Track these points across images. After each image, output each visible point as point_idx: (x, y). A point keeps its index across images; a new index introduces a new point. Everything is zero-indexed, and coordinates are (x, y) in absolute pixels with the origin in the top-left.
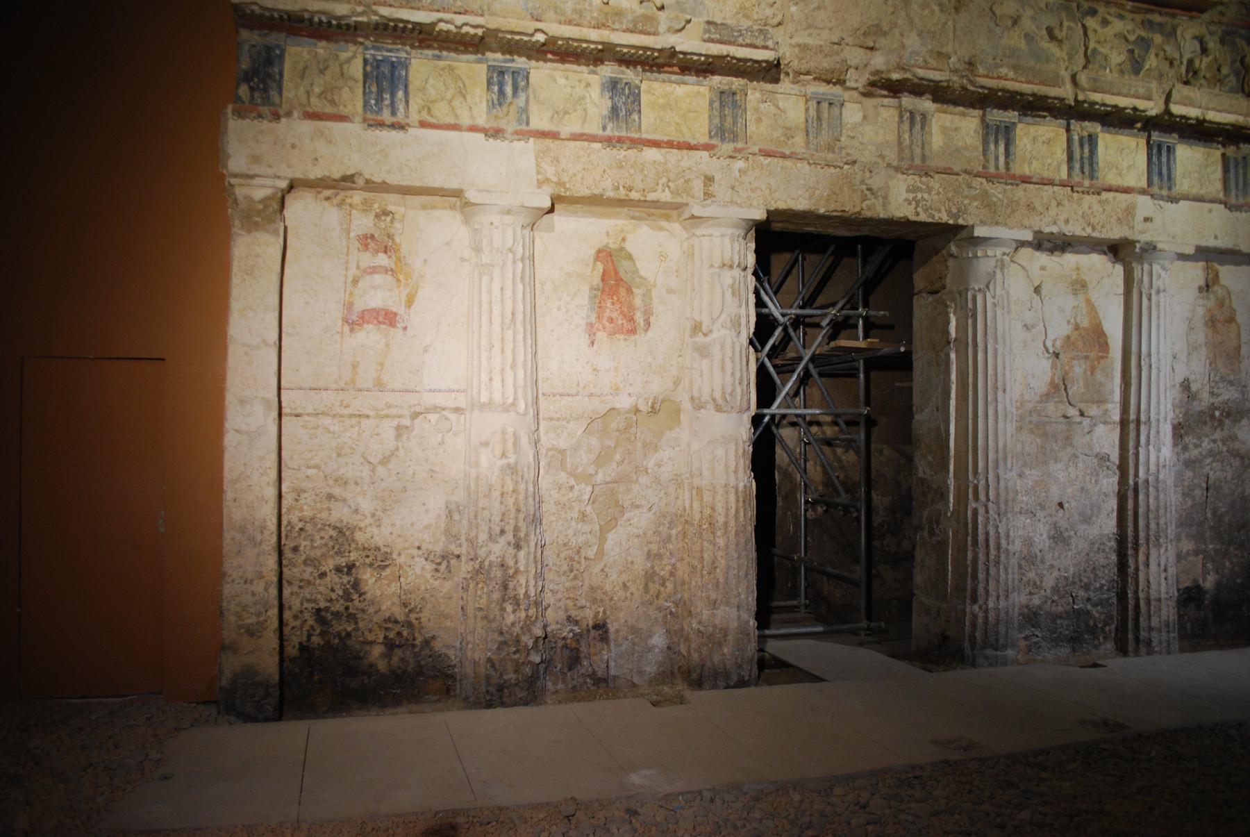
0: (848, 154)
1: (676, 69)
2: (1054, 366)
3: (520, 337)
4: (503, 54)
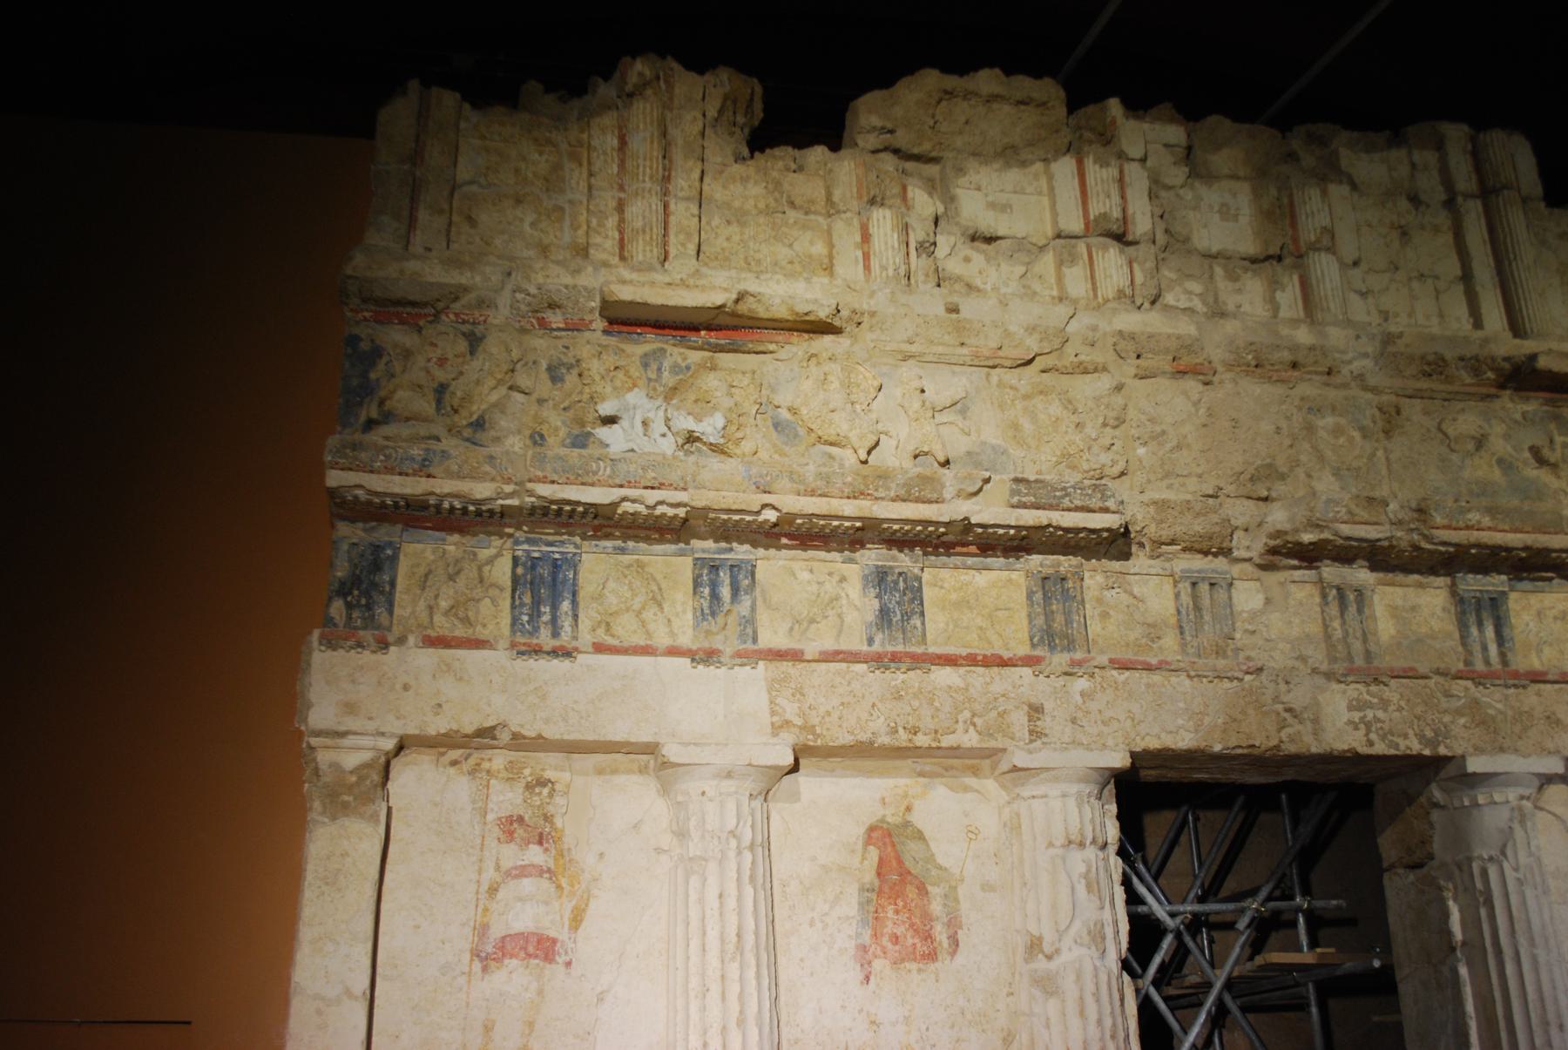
0: (1248, 658)
1: (973, 549)
3: (751, 974)
4: (716, 541)
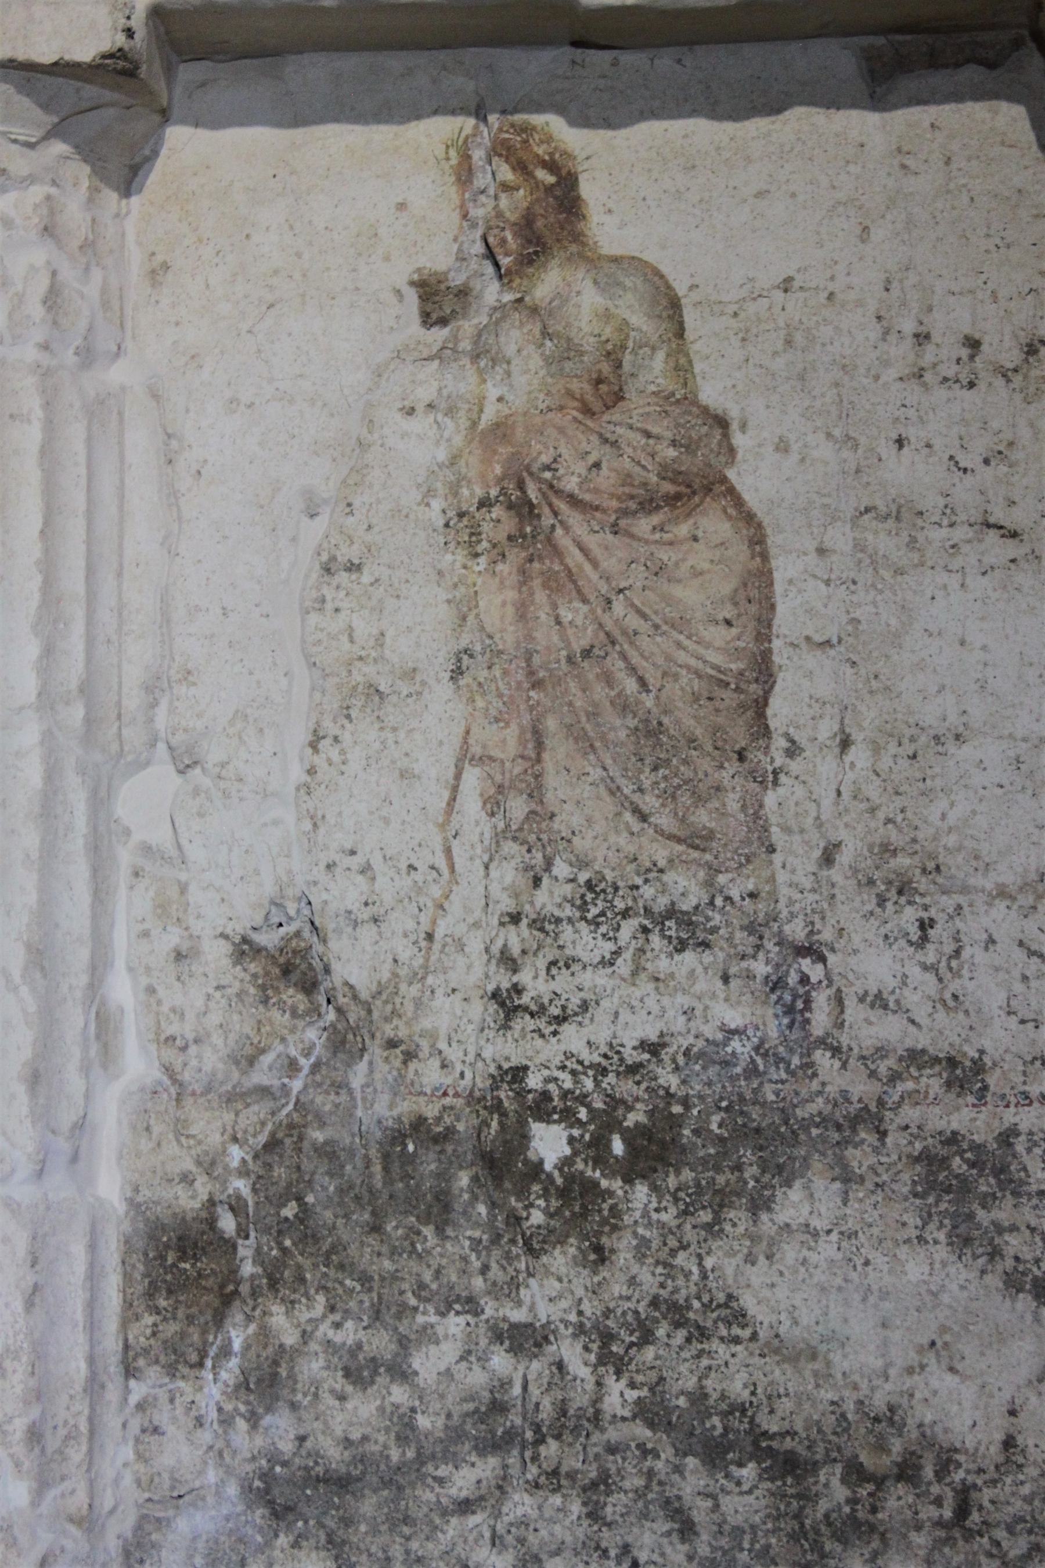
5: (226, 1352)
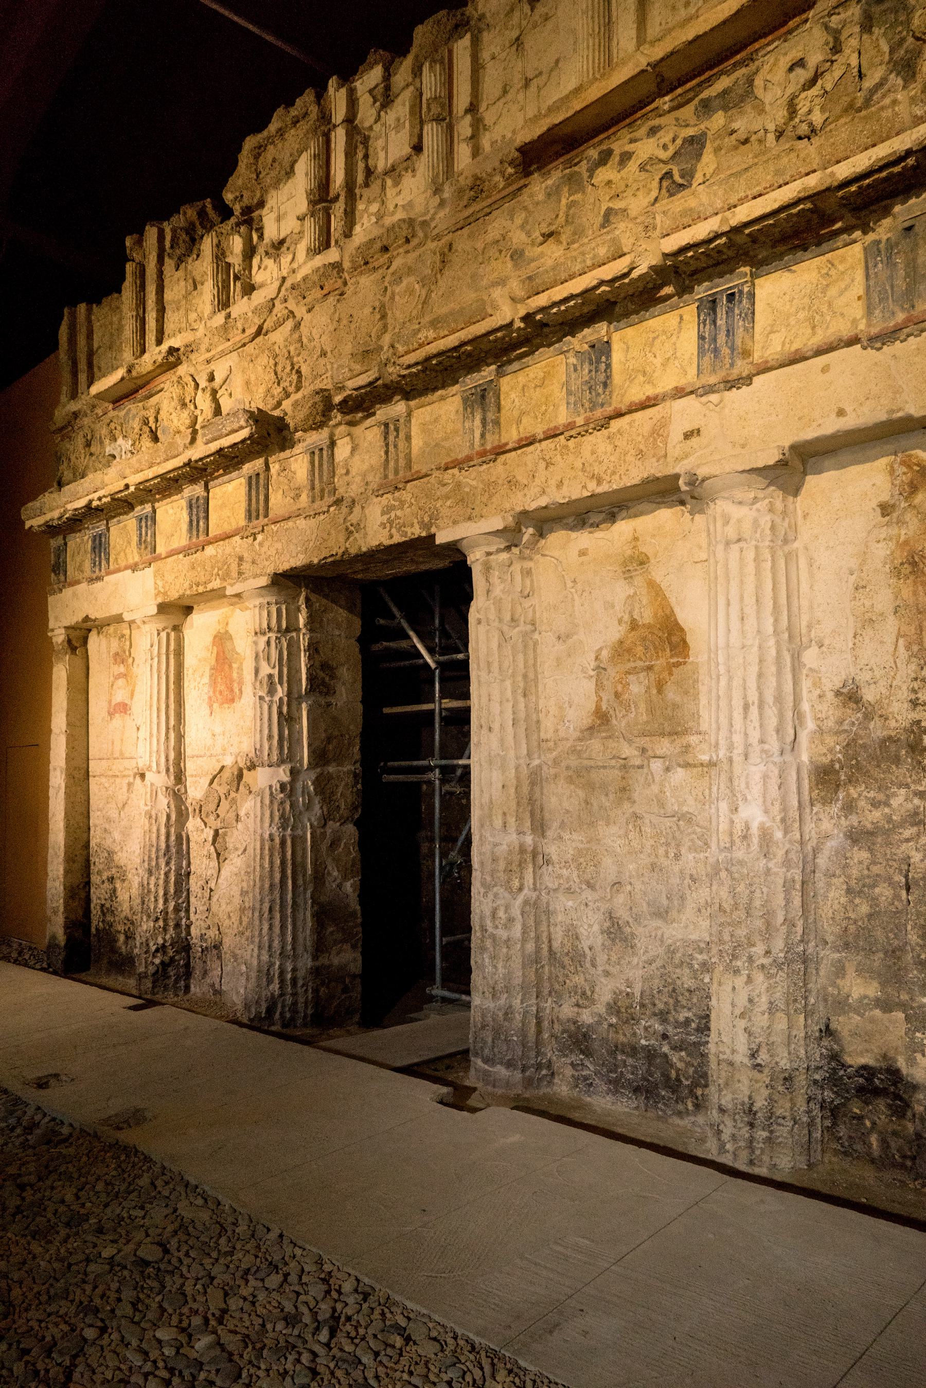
2: (599, 686)
5: (838, 800)
